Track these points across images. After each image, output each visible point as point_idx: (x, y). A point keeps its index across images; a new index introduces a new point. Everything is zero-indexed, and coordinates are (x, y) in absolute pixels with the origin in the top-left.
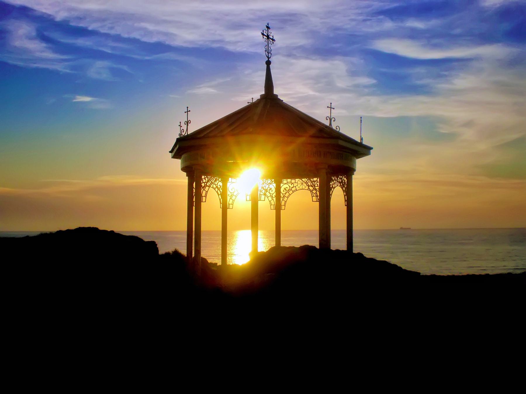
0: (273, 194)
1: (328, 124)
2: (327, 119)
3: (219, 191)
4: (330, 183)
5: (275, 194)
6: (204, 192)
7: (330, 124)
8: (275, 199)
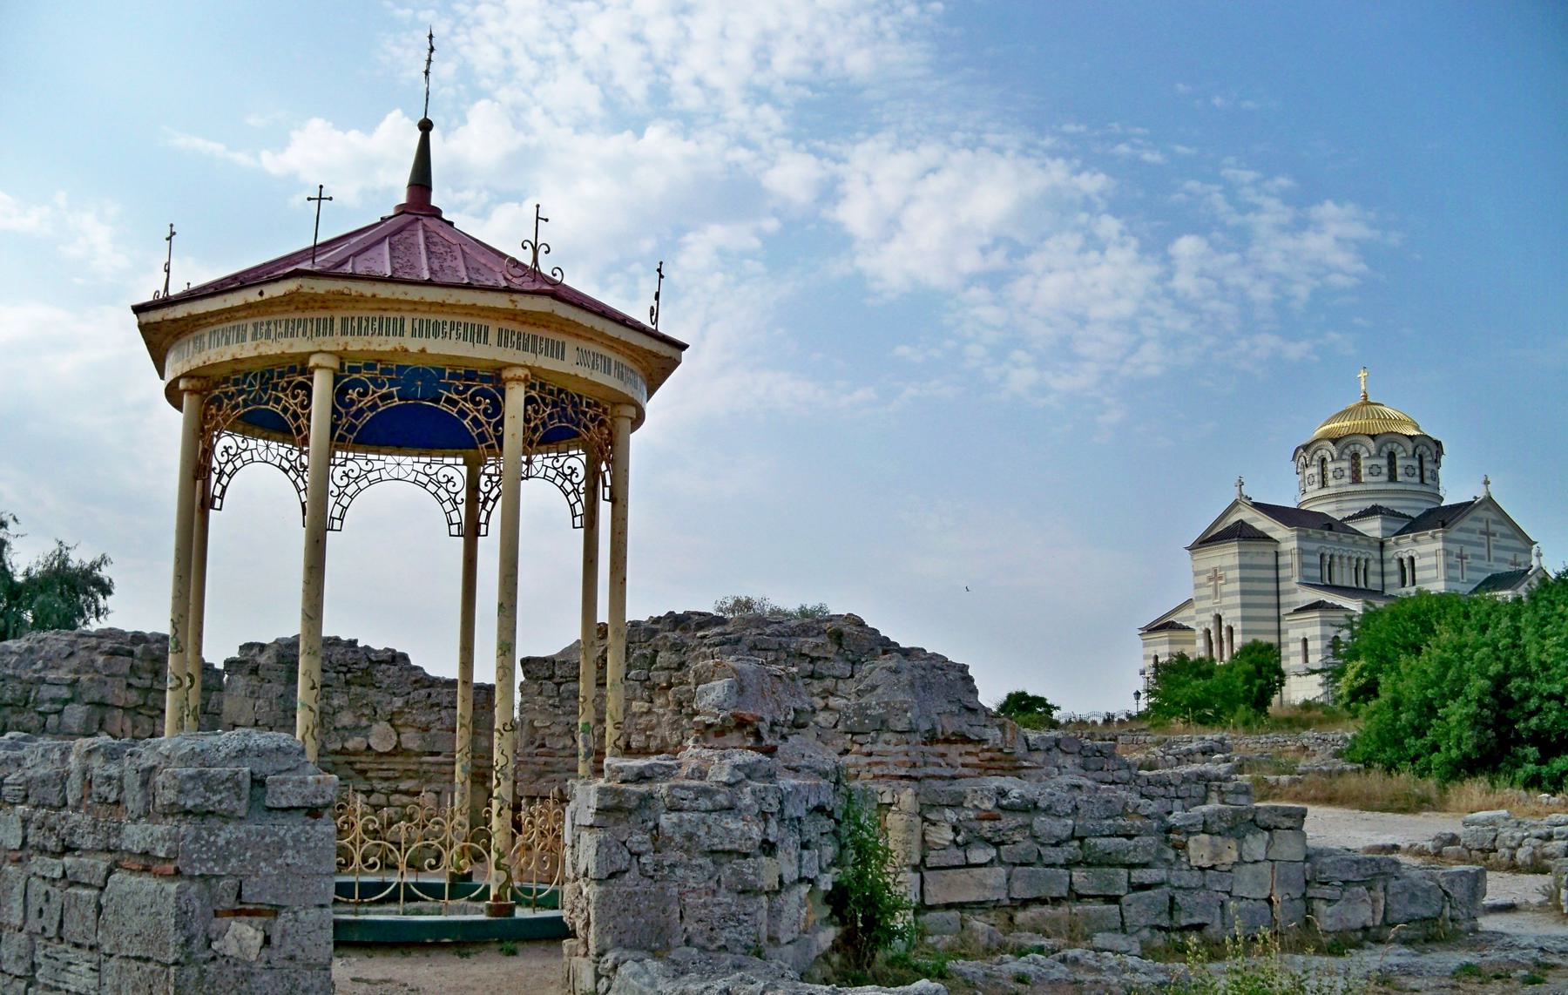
0: (456, 493)
1: (528, 261)
2: (525, 248)
3: (299, 481)
4: (586, 452)
5: (463, 495)
6: (484, 514)
7: (535, 260)
8: (462, 508)
